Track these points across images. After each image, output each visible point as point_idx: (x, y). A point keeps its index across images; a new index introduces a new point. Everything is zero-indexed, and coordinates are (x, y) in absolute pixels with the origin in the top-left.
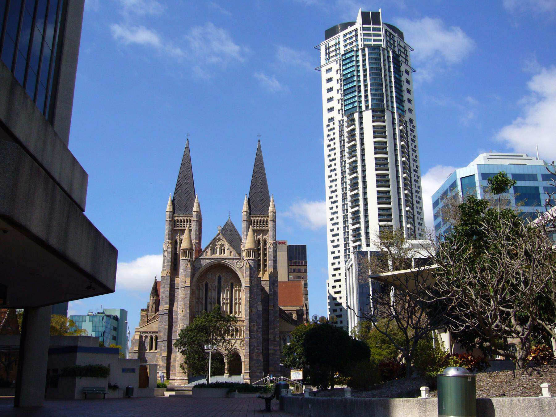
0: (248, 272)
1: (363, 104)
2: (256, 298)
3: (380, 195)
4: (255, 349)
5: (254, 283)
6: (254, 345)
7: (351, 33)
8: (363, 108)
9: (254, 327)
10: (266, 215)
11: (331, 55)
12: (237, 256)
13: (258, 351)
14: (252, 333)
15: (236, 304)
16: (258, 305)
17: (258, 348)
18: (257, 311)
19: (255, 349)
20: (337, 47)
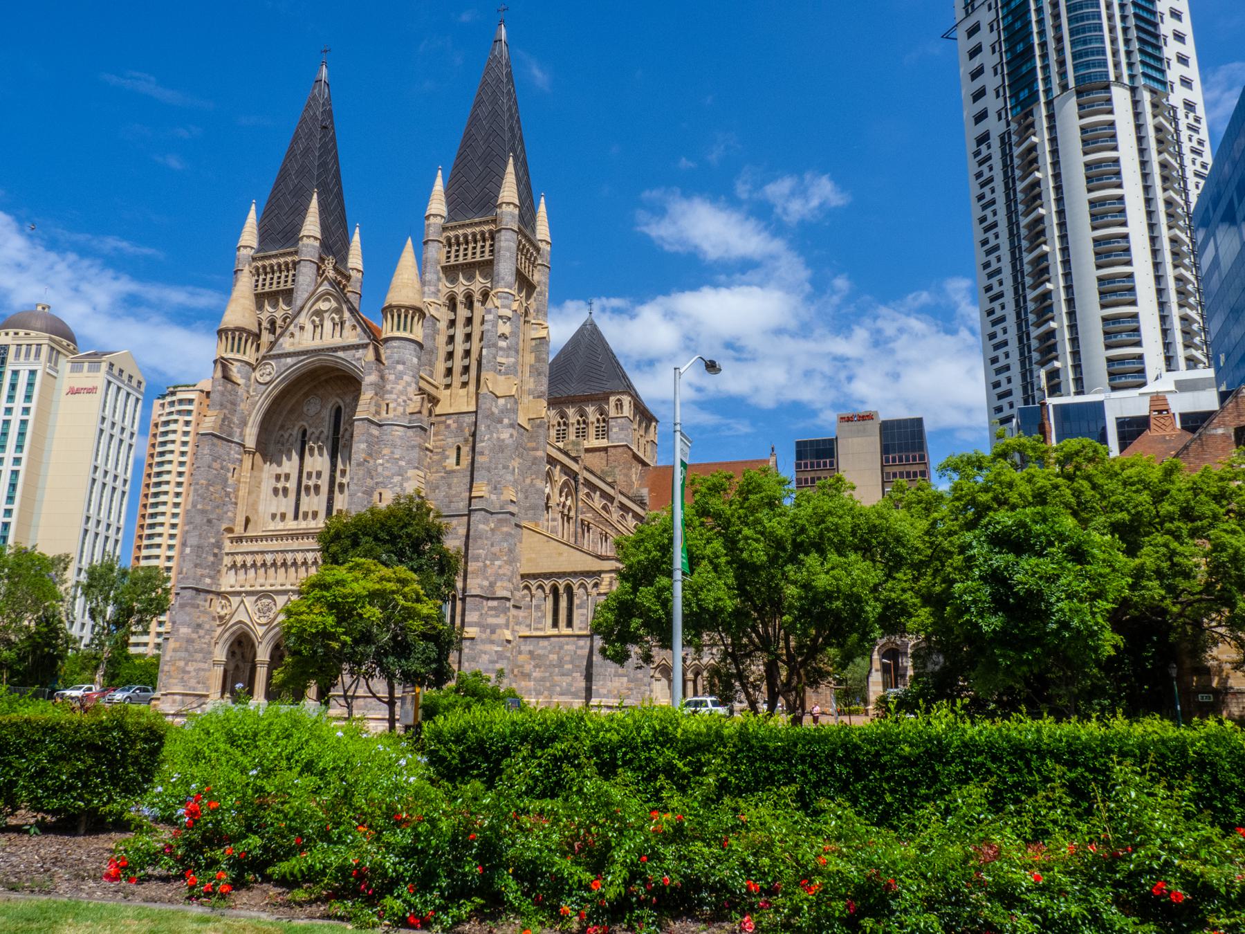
0: (370, 374)
1: (1055, 80)
2: (400, 459)
3: (1128, 298)
5: (395, 410)
8: (1056, 91)
16: (408, 479)
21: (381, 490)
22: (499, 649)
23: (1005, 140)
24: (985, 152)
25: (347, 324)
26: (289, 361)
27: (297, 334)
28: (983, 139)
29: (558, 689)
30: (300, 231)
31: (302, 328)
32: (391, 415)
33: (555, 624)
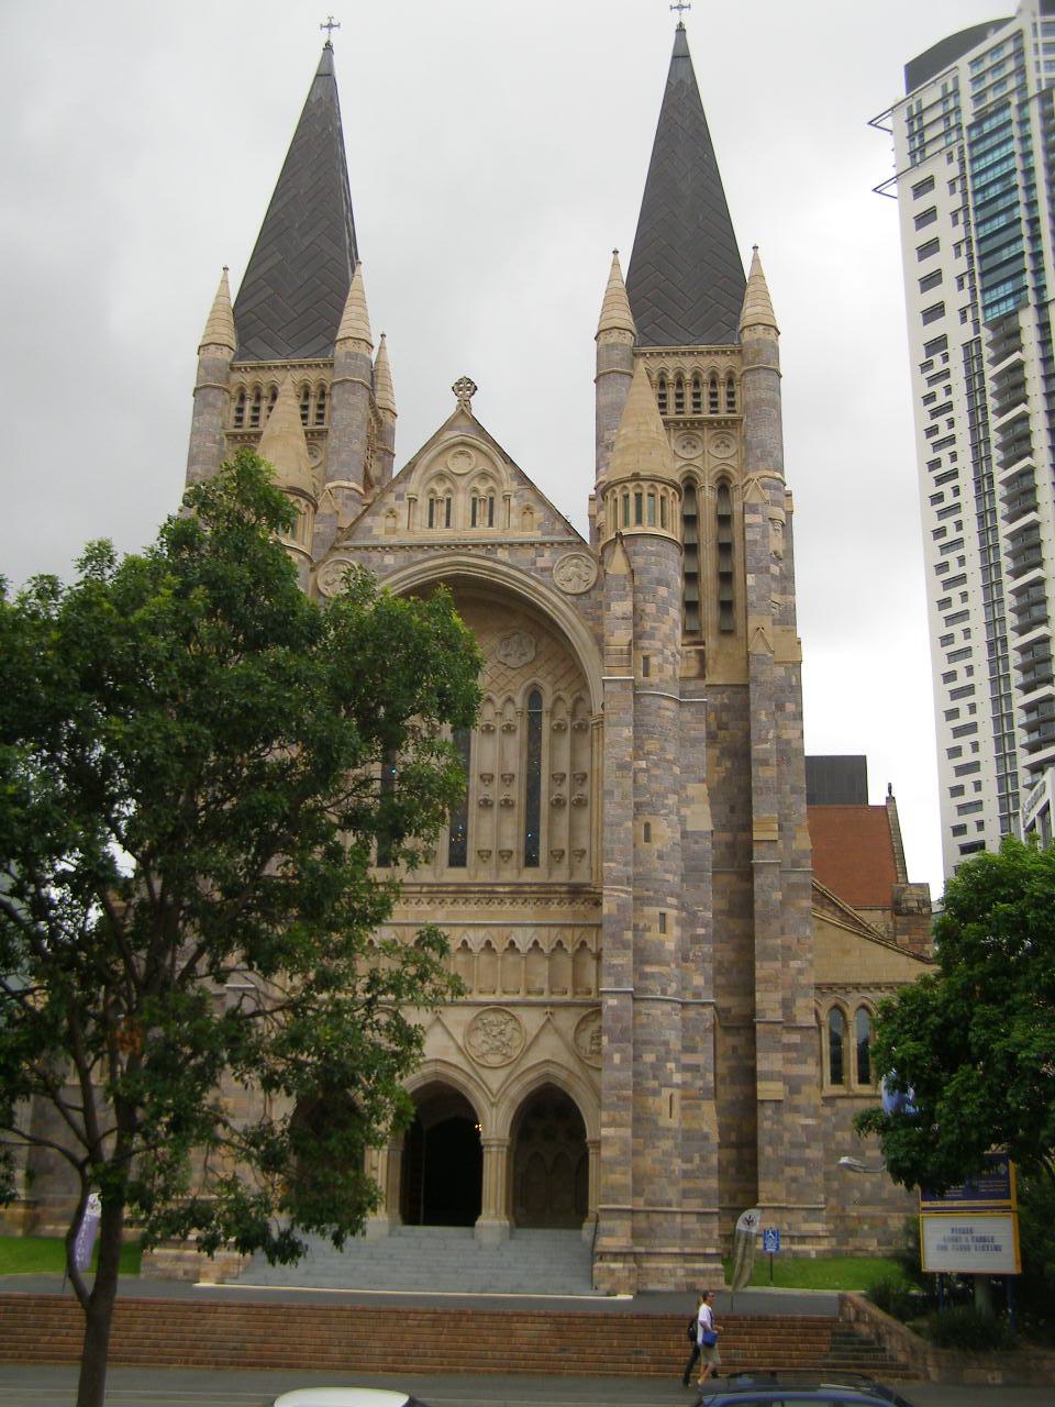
0: (622, 598)
2: (673, 762)
4: (671, 1065)
5: (661, 669)
6: (666, 1043)
7: (998, 48)
9: (663, 930)
10: (724, 347)
11: (928, 136)
12: (560, 534)
13: (688, 1076)
14: (648, 969)
15: (558, 804)
17: (688, 1059)
18: (685, 834)
19: (671, 1065)
20: (951, 105)
21: (648, 818)
22: (810, 1122)
23: (971, 351)
24: (939, 366)
25: (514, 502)
26: (389, 560)
27: (403, 513)
28: (937, 345)
29: (857, 1194)
30: (336, 324)
31: (412, 501)
32: (654, 678)
33: (837, 1077)
